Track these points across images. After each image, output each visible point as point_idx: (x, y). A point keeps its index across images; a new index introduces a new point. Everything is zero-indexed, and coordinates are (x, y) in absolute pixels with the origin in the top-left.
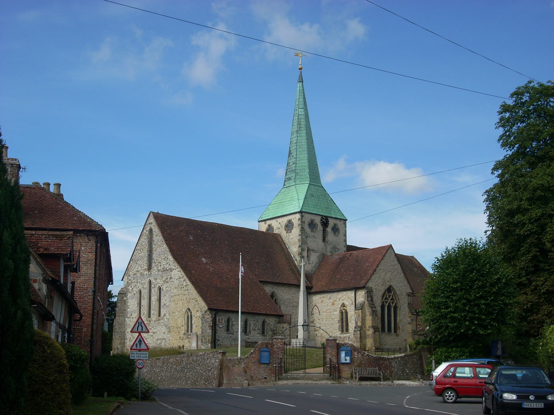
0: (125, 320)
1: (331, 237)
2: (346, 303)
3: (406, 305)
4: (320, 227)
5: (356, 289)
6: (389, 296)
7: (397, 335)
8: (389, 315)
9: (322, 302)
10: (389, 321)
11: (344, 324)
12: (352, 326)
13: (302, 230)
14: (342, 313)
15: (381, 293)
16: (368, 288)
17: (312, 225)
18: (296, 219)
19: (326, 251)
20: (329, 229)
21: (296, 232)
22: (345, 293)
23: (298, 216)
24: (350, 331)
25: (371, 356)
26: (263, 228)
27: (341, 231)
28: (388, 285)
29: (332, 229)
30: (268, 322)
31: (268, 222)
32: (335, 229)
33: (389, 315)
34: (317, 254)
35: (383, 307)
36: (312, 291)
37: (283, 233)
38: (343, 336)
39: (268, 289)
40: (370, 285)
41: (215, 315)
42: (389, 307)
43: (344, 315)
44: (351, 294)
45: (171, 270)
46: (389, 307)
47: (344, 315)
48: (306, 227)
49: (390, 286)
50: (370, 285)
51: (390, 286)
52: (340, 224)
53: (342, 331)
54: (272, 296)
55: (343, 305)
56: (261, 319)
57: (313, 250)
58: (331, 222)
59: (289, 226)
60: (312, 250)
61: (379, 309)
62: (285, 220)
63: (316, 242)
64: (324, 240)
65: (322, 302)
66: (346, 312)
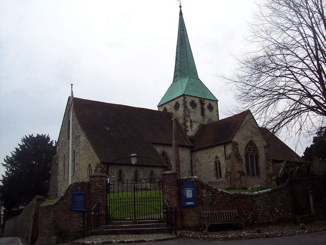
0: (57, 178)
1: (207, 112)
2: (219, 155)
3: (264, 155)
4: (199, 106)
5: (225, 144)
6: (251, 148)
7: (259, 178)
8: (252, 163)
9: (202, 156)
10: (252, 167)
11: (218, 171)
12: (224, 172)
13: (185, 107)
14: (216, 164)
15: (244, 146)
16: (234, 142)
17: (193, 104)
18: (181, 101)
19: (204, 122)
20: (205, 107)
21: (181, 109)
22: (217, 148)
23: (182, 98)
24: (223, 177)
25: (226, 193)
26: (162, 110)
27: (215, 109)
28: (249, 139)
29: (208, 107)
30: (155, 172)
31: (164, 106)
32: (210, 108)
33: (252, 163)
34: (198, 124)
35: (247, 156)
36: (195, 149)
37: (173, 111)
38: (217, 180)
39: (159, 149)
40: (235, 139)
41: (108, 168)
42: (252, 156)
43: (218, 165)
44: (221, 148)
45: (80, 136)
46: (252, 156)
47: (218, 165)
48: (188, 105)
49: (251, 141)
50: (235, 139)
51: (251, 141)
52: (213, 104)
53: (217, 177)
54: (164, 154)
55: (217, 157)
56: (149, 170)
57: (194, 122)
58: (207, 103)
59: (177, 107)
60: (194, 122)
61: (243, 158)
62: (174, 103)
63: (196, 115)
64: (203, 114)
65: (202, 156)
66: (219, 163)
